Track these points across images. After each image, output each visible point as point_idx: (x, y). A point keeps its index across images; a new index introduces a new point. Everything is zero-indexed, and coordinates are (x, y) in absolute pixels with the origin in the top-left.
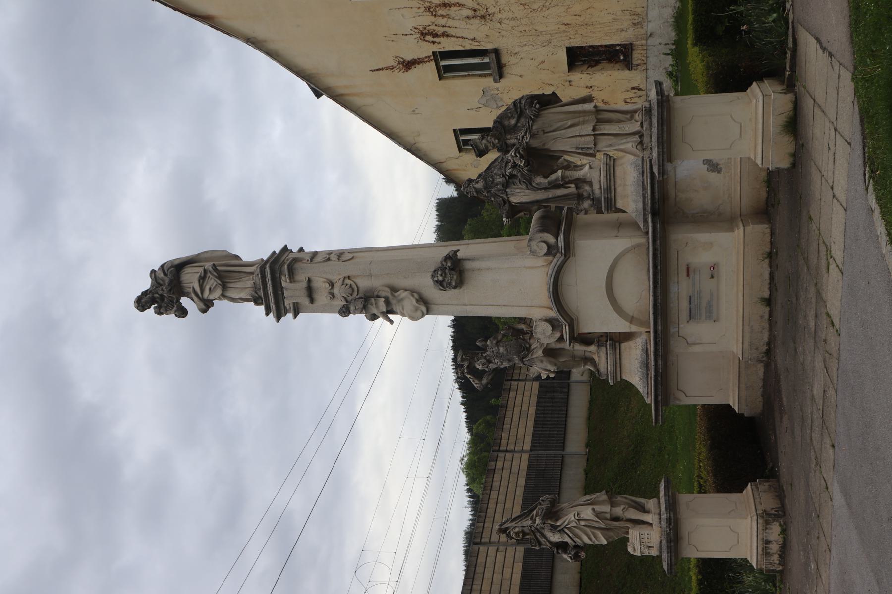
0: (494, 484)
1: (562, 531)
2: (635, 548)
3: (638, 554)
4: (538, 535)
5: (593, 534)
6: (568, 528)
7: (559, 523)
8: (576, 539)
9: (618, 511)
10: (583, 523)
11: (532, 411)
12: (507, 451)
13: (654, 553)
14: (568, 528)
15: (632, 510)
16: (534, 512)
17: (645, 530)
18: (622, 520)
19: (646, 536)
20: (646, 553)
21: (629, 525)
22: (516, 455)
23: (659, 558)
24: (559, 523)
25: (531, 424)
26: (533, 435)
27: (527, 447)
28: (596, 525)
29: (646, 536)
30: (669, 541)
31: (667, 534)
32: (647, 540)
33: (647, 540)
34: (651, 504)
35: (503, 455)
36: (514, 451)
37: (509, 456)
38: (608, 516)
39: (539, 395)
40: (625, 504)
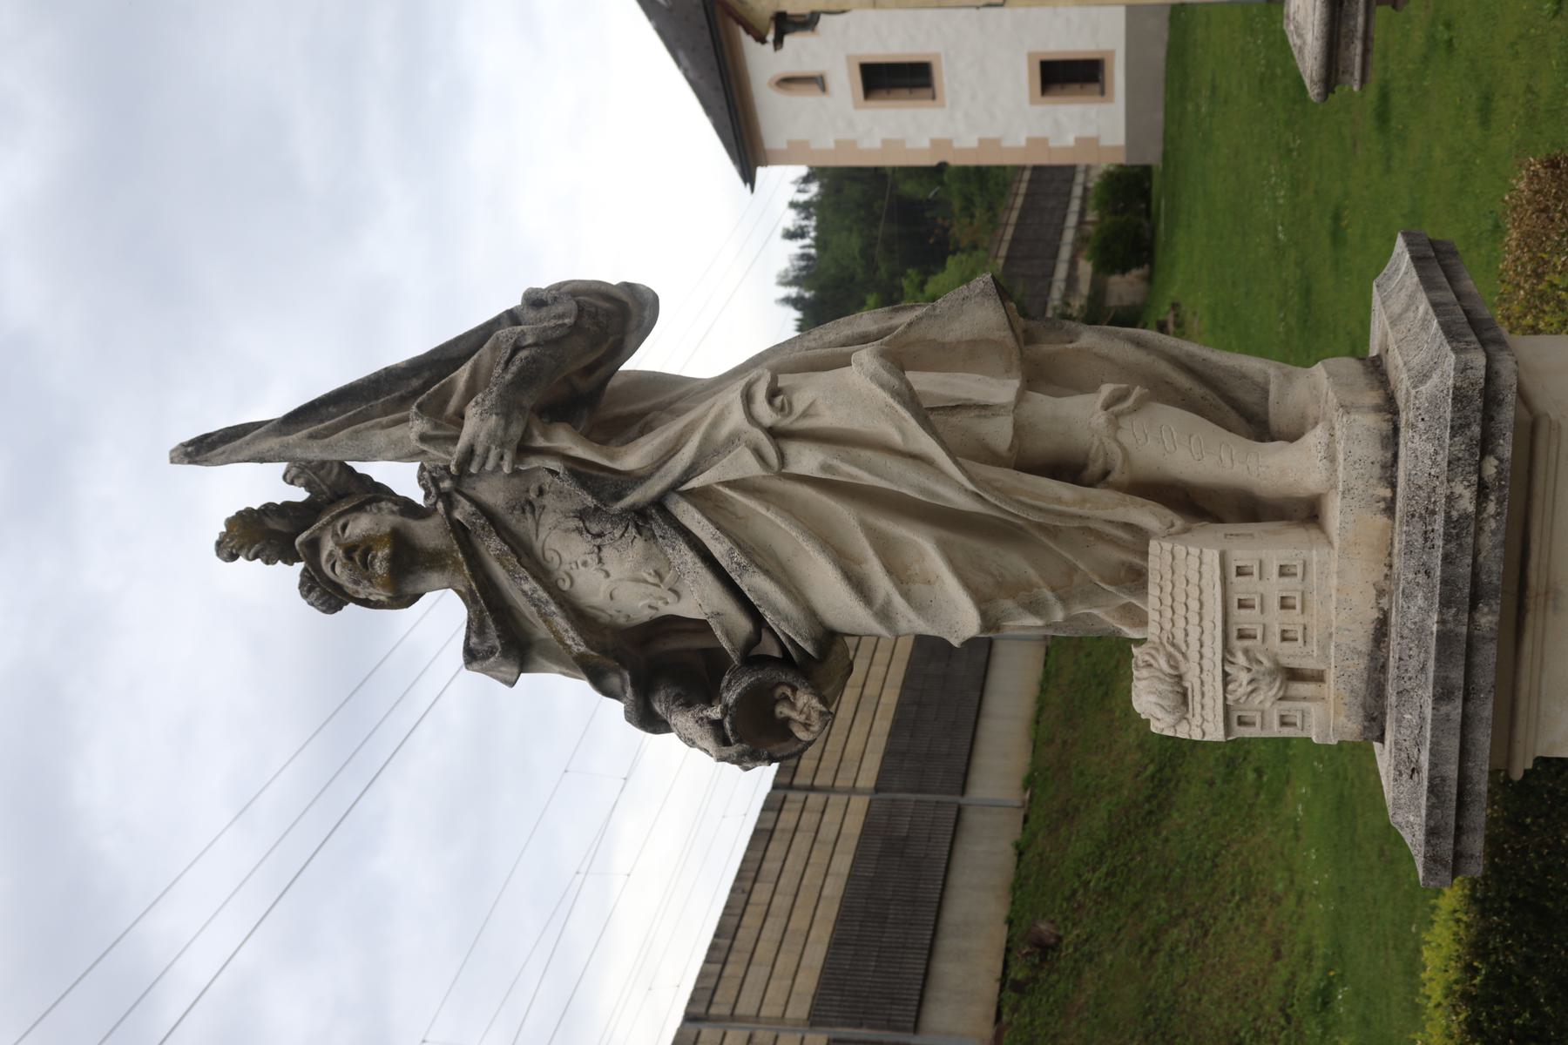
0: (766, 865)
1: (652, 518)
2: (1182, 691)
3: (1206, 726)
4: (491, 547)
5: (886, 549)
6: (704, 499)
7: (632, 458)
8: (756, 584)
9: (1079, 416)
10: (807, 460)
11: (891, 698)
12: (812, 788)
13: (1325, 718)
14: (704, 499)
15: (1172, 419)
16: (462, 374)
17: (1265, 549)
18: (1103, 479)
19: (1275, 587)
20: (1267, 716)
21: (1147, 516)
22: (833, 798)
23: (1347, 768)
24: (632, 458)
25: (883, 725)
26: (888, 753)
27: (868, 779)
28: (906, 481)
29: (1275, 587)
30: (1463, 593)
31: (1455, 529)
32: (1276, 619)
33: (1276, 619)
34: (1317, 386)
35: (800, 796)
36: (831, 789)
37: (815, 799)
38: (1000, 433)
39: (910, 663)
40: (1128, 372)
